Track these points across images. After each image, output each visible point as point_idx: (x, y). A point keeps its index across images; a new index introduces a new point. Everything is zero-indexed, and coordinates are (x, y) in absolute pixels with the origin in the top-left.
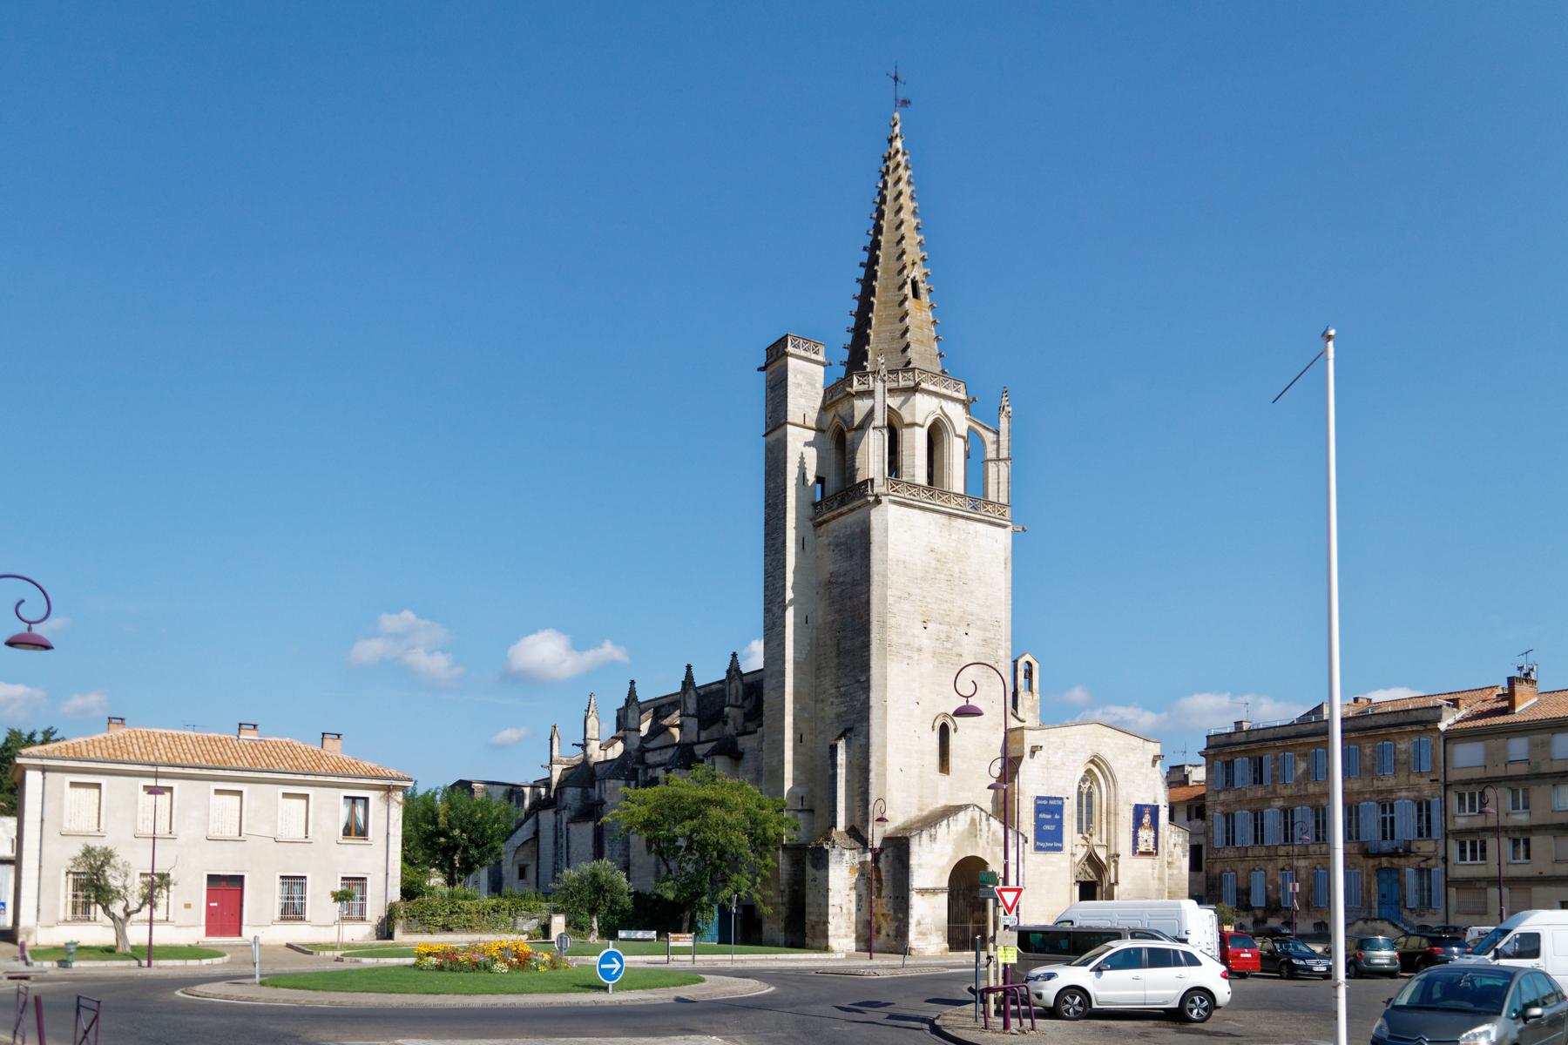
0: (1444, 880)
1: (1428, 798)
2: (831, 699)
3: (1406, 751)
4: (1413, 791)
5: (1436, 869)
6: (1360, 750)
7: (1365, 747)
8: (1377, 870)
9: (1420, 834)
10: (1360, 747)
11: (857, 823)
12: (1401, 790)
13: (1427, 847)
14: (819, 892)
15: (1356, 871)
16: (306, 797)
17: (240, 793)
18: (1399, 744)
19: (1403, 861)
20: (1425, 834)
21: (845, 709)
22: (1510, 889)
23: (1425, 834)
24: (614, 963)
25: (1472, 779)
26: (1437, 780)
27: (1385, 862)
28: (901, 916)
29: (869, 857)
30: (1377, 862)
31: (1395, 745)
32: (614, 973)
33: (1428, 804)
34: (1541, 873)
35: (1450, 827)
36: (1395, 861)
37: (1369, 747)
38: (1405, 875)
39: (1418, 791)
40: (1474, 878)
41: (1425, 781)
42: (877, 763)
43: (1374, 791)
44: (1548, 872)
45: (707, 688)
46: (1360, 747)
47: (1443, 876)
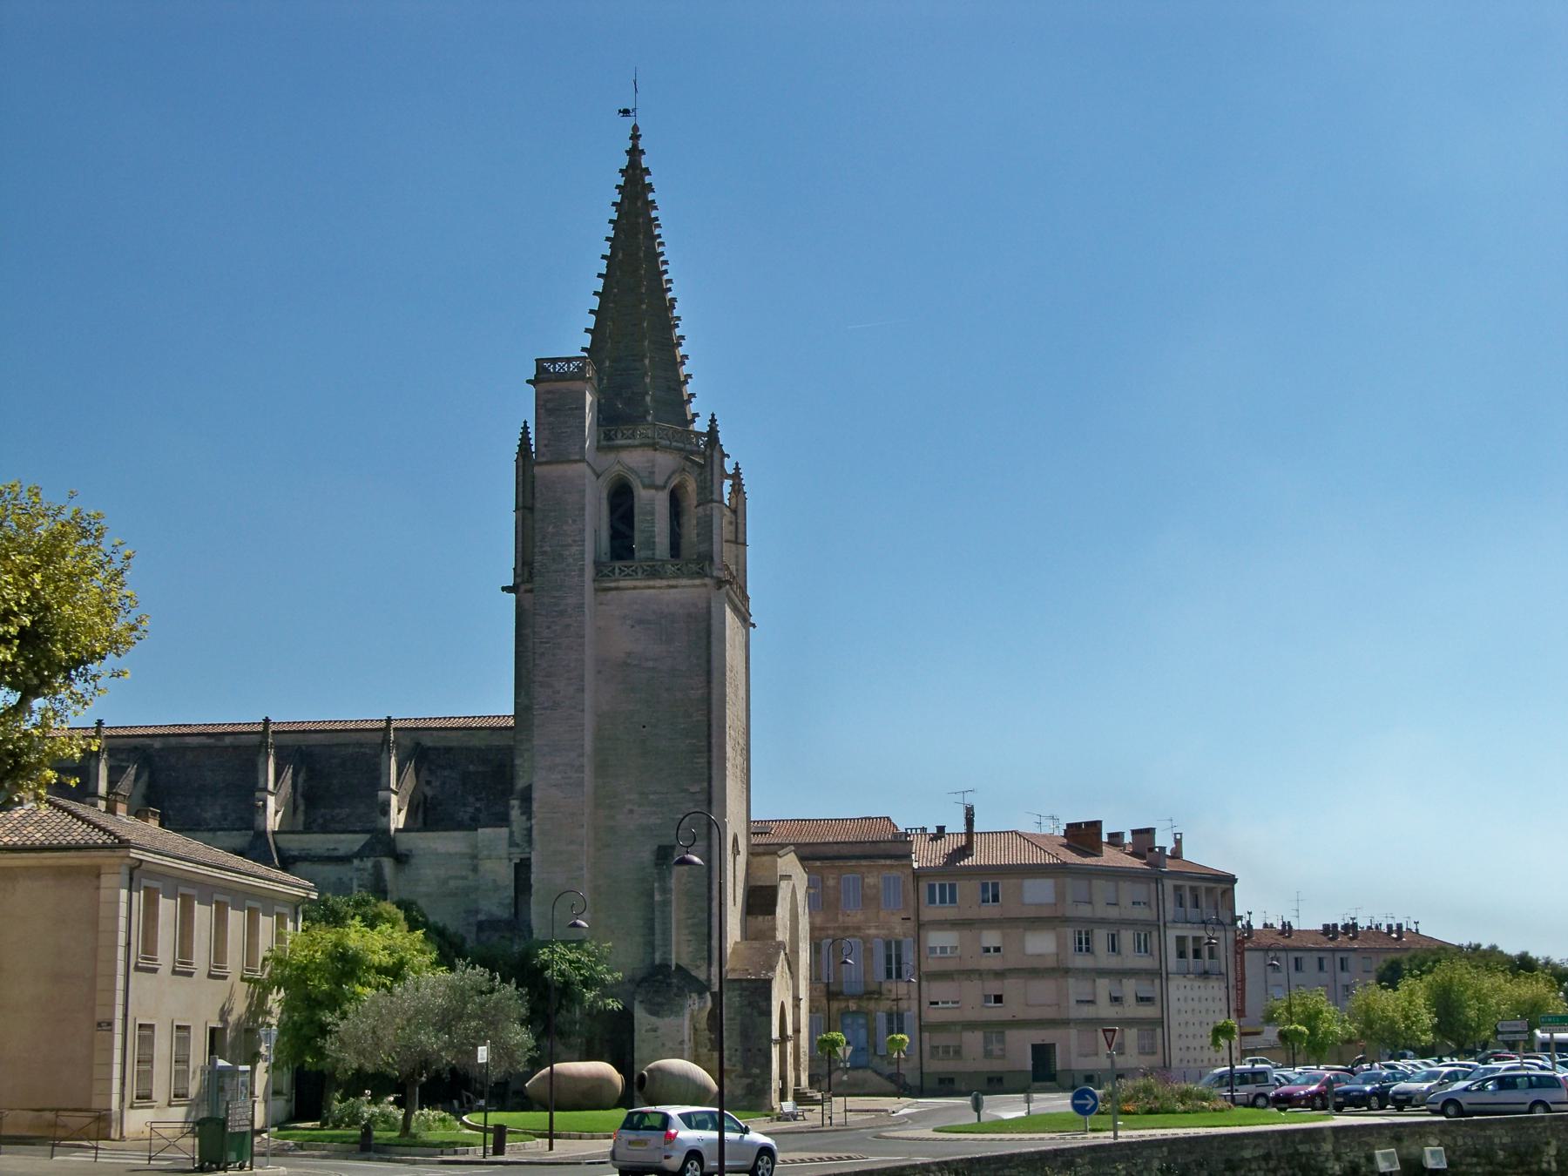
0: (917, 1025)
1: (901, 938)
2: (629, 806)
3: (875, 886)
4: (883, 929)
5: (909, 1013)
6: (823, 881)
7: (828, 879)
8: (842, 1014)
9: (889, 975)
10: (823, 878)
11: (682, 963)
12: (869, 928)
13: (901, 988)
14: (663, 1045)
15: (818, 1015)
16: (1370, 958)
17: (1370, 958)
18: (868, 877)
19: (872, 1005)
20: (894, 976)
21: (659, 821)
22: (1078, 1030)
23: (894, 976)
24: (1087, 1099)
25: (946, 920)
26: (909, 919)
27: (853, 1006)
28: (756, 1071)
29: (709, 1004)
30: (843, 1005)
31: (863, 879)
32: (1088, 1108)
33: (899, 944)
34: (1014, 1016)
35: (924, 968)
36: (864, 1004)
37: (833, 878)
38: (875, 1020)
39: (888, 929)
40: (948, 1022)
41: (896, 919)
42: (782, 897)
43: (839, 928)
44: (1021, 1016)
45: (173, 741)
46: (823, 878)
47: (917, 1021)
